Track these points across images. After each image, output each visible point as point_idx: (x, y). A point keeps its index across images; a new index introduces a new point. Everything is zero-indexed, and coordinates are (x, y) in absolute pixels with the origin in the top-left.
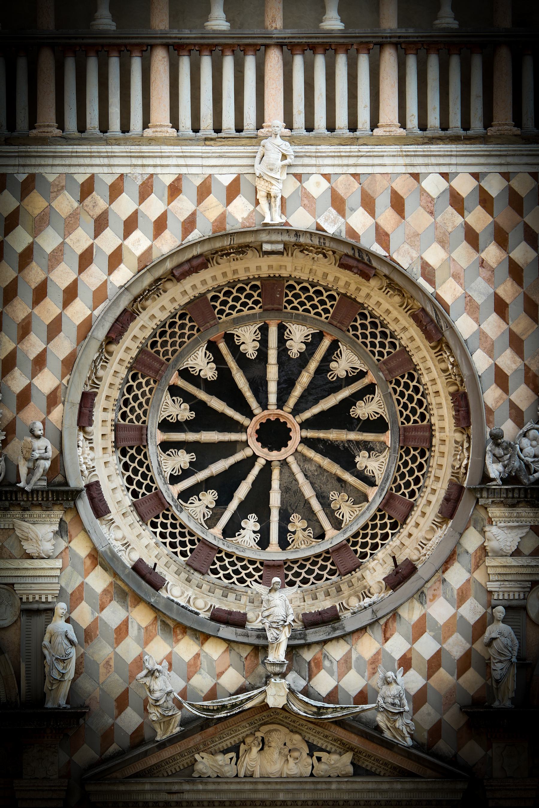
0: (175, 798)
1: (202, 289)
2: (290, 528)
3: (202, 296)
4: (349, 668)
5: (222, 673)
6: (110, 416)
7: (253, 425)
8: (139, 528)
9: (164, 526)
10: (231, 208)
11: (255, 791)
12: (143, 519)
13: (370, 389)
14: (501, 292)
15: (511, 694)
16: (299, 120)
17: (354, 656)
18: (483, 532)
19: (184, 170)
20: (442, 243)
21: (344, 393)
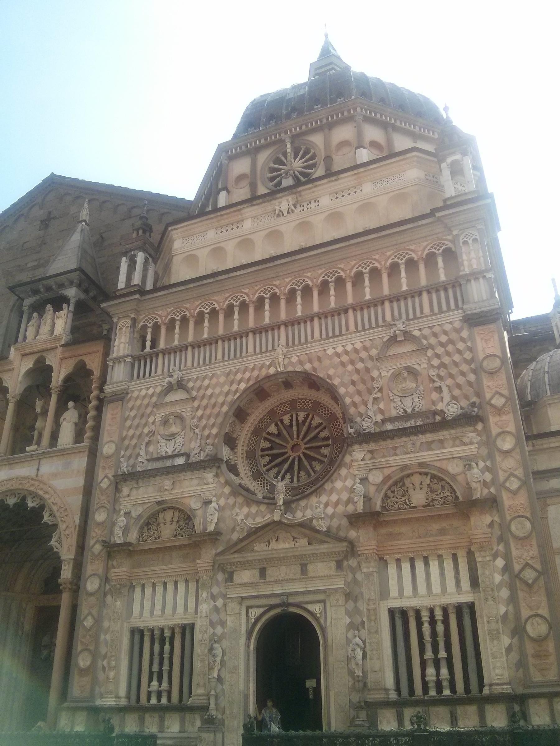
0: (245, 560)
1: (272, 407)
2: (300, 476)
3: (273, 409)
4: (307, 509)
5: (265, 516)
6: (245, 448)
7: (289, 446)
8: (252, 481)
9: (261, 481)
10: (269, 371)
11: (272, 554)
12: (255, 480)
13: (324, 428)
14: (353, 378)
15: (362, 508)
16: (290, 343)
17: (309, 504)
18: (351, 455)
19: (256, 363)
20: (333, 368)
21: (317, 431)
